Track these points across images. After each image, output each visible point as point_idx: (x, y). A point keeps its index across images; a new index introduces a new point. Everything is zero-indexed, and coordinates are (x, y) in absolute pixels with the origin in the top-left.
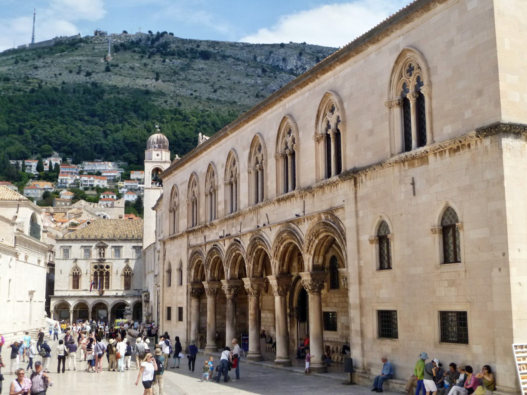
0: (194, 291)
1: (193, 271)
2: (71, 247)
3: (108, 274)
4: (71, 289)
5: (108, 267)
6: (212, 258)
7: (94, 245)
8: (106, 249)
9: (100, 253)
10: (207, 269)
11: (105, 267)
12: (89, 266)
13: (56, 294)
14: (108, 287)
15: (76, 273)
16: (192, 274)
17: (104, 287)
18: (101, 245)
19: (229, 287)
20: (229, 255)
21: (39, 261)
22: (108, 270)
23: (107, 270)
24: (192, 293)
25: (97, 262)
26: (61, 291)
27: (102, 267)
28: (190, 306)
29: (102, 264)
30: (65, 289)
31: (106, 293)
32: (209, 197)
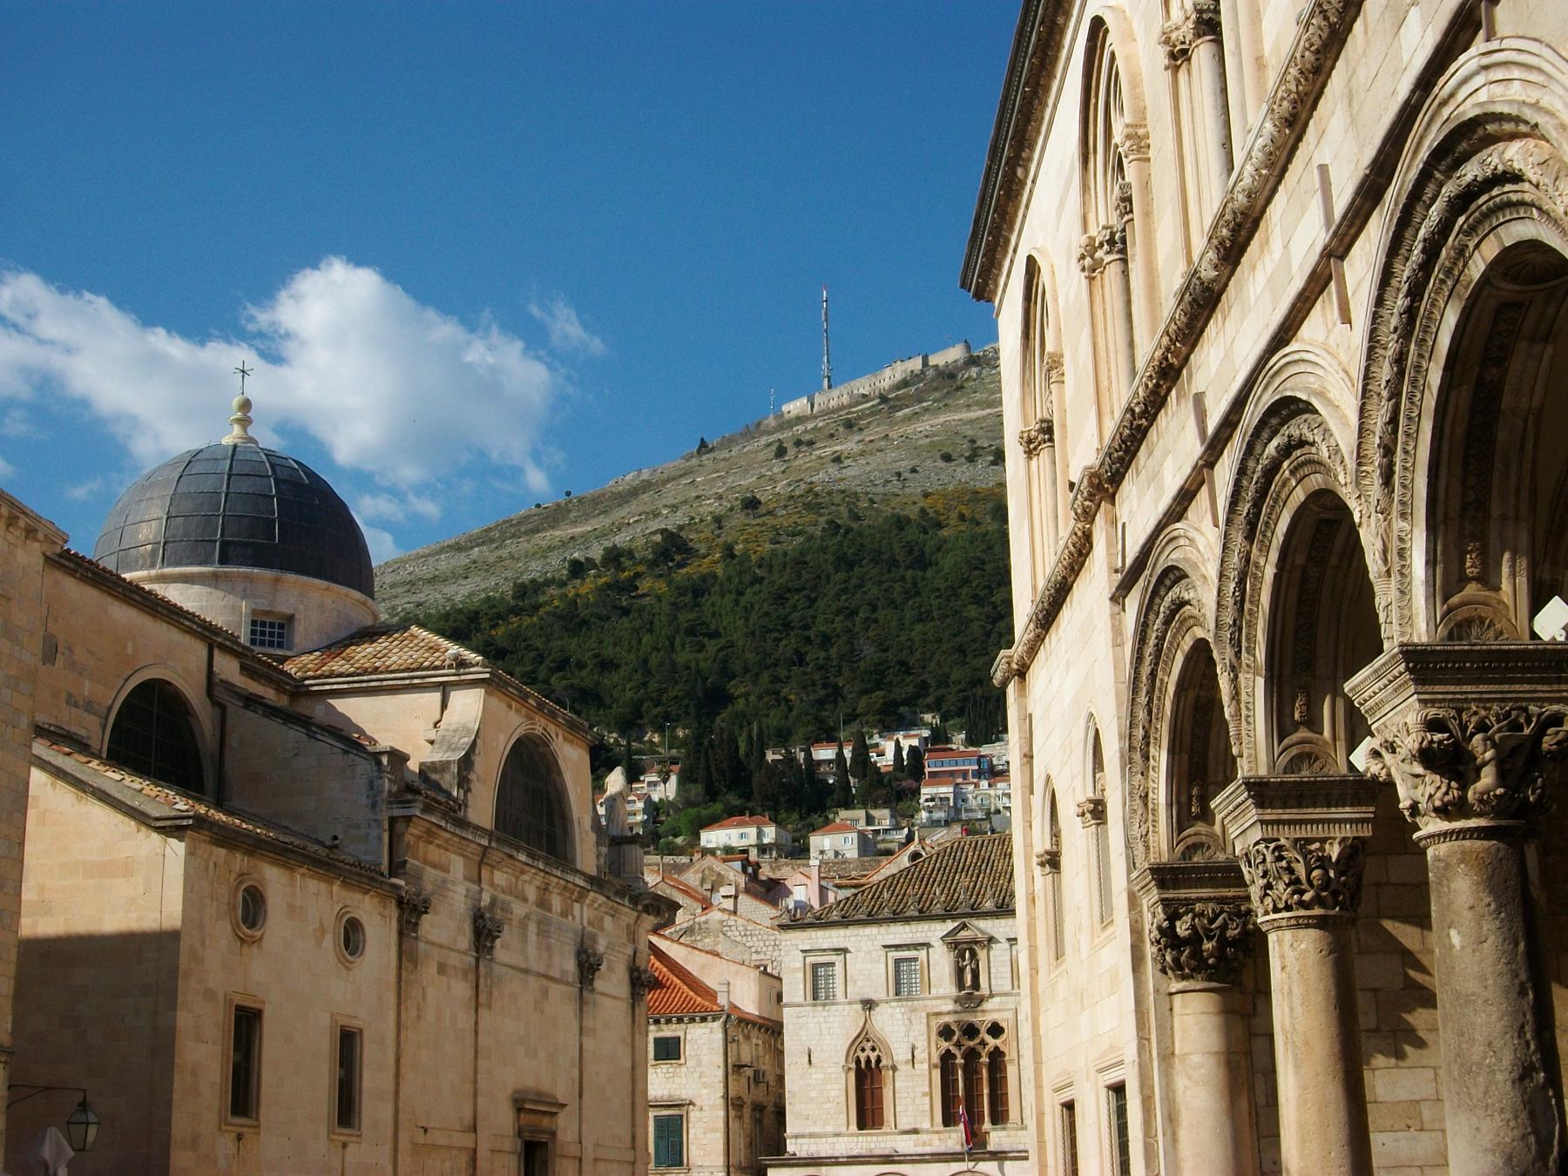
0: (1182, 928)
1: (1161, 758)
2: (844, 951)
3: (997, 1055)
4: (854, 1127)
5: (996, 1030)
6: (1265, 549)
7: (935, 932)
8: (982, 954)
9: (960, 972)
10: (1234, 670)
11: (983, 1030)
12: (920, 1027)
13: (791, 1146)
14: (999, 1117)
15: (868, 1061)
16: (1160, 794)
17: (987, 1119)
18: (963, 934)
19: (1432, 725)
20: (1400, 359)
21: (588, 966)
22: (998, 1042)
23: (992, 1042)
24: (1168, 936)
25: (950, 1006)
26: (811, 1136)
27: (971, 1031)
28: (1167, 1056)
29: (970, 1018)
30: (830, 1129)
31: (997, 1138)
32: (1202, 53)
